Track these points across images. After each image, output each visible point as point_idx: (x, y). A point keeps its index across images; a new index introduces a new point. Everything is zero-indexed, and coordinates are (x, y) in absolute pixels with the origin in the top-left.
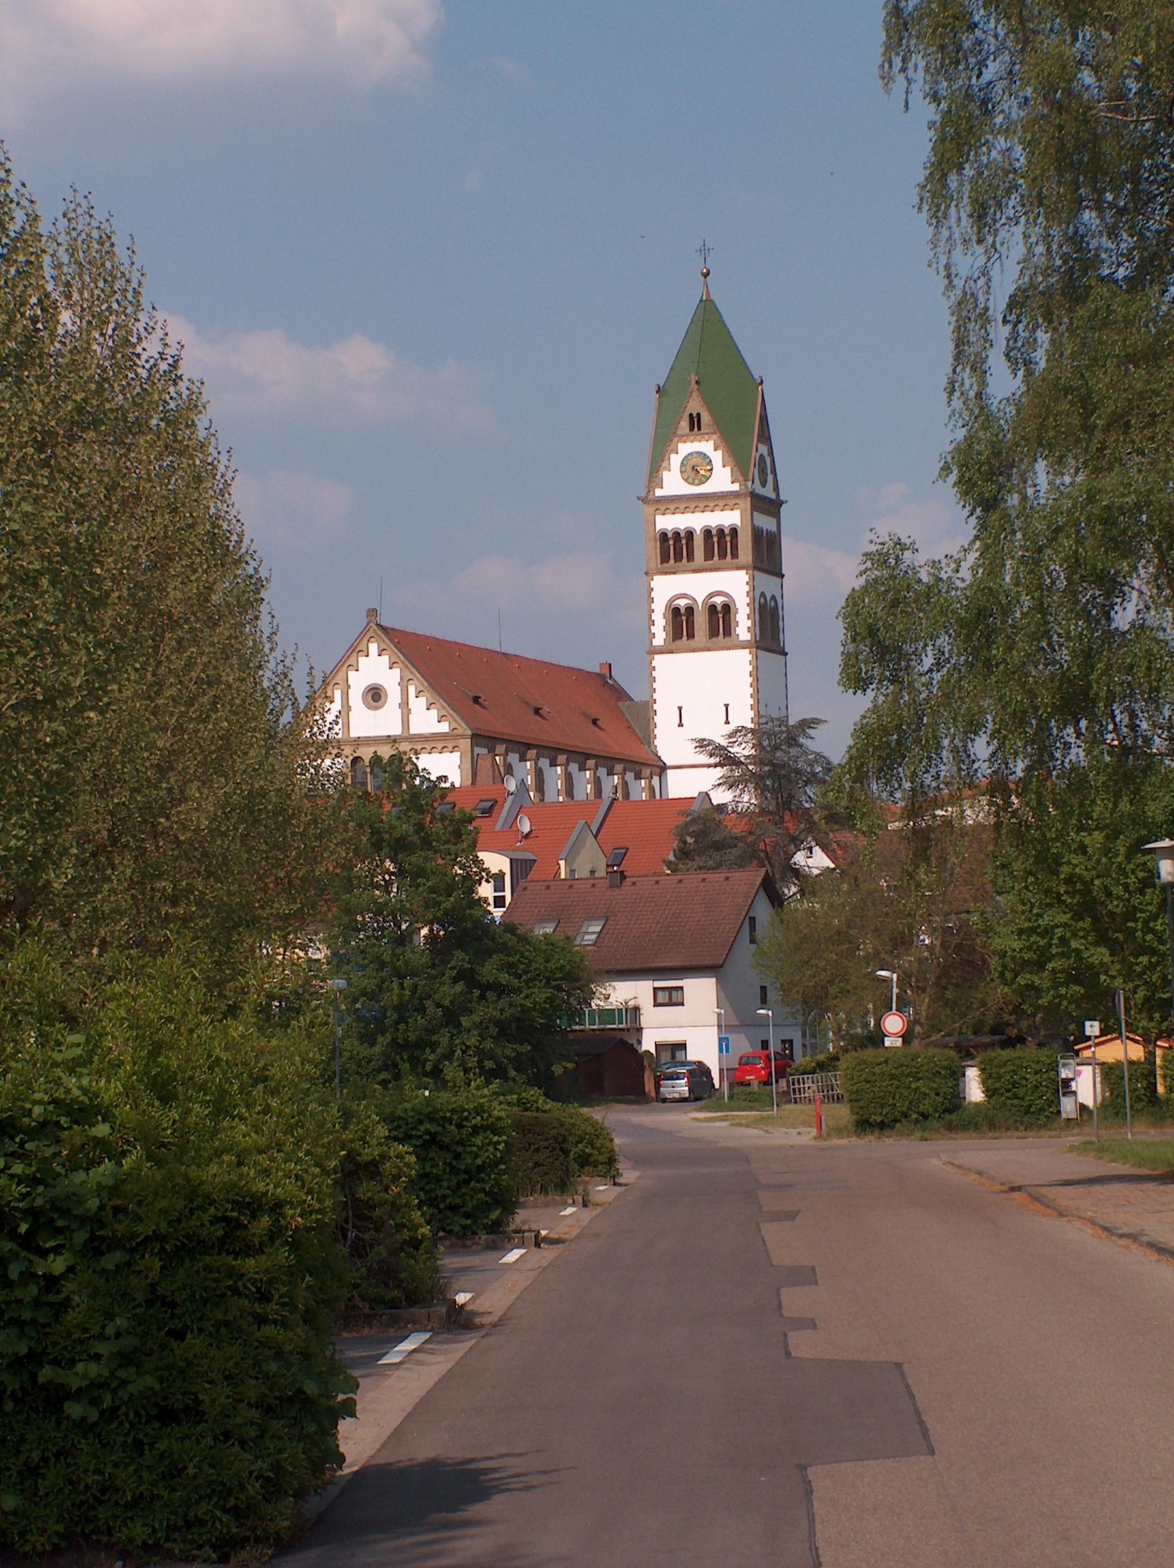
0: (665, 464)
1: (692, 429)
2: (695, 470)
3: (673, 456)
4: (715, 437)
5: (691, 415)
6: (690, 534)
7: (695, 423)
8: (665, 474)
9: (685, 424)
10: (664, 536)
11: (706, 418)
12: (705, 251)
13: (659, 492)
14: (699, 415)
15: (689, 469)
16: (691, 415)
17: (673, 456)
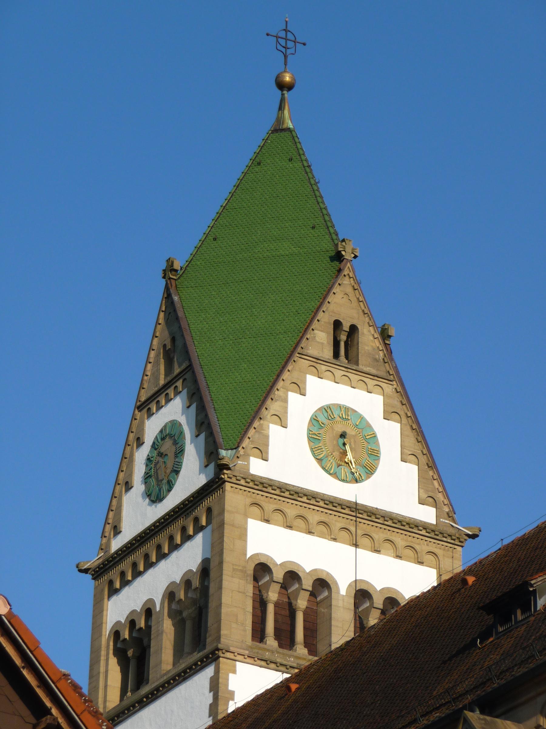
0: (273, 406)
1: (336, 355)
2: (341, 442)
3: (293, 397)
4: (389, 388)
5: (337, 324)
6: (322, 584)
7: (345, 346)
8: (274, 431)
9: (320, 339)
10: (262, 569)
11: (368, 341)
12: (286, 42)
13: (257, 467)
14: (353, 329)
15: (328, 440)
16: (337, 324)
17: (293, 397)
